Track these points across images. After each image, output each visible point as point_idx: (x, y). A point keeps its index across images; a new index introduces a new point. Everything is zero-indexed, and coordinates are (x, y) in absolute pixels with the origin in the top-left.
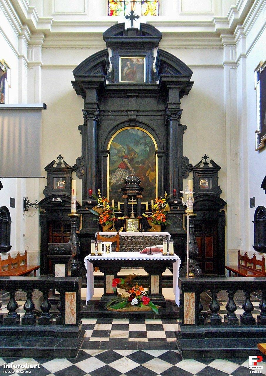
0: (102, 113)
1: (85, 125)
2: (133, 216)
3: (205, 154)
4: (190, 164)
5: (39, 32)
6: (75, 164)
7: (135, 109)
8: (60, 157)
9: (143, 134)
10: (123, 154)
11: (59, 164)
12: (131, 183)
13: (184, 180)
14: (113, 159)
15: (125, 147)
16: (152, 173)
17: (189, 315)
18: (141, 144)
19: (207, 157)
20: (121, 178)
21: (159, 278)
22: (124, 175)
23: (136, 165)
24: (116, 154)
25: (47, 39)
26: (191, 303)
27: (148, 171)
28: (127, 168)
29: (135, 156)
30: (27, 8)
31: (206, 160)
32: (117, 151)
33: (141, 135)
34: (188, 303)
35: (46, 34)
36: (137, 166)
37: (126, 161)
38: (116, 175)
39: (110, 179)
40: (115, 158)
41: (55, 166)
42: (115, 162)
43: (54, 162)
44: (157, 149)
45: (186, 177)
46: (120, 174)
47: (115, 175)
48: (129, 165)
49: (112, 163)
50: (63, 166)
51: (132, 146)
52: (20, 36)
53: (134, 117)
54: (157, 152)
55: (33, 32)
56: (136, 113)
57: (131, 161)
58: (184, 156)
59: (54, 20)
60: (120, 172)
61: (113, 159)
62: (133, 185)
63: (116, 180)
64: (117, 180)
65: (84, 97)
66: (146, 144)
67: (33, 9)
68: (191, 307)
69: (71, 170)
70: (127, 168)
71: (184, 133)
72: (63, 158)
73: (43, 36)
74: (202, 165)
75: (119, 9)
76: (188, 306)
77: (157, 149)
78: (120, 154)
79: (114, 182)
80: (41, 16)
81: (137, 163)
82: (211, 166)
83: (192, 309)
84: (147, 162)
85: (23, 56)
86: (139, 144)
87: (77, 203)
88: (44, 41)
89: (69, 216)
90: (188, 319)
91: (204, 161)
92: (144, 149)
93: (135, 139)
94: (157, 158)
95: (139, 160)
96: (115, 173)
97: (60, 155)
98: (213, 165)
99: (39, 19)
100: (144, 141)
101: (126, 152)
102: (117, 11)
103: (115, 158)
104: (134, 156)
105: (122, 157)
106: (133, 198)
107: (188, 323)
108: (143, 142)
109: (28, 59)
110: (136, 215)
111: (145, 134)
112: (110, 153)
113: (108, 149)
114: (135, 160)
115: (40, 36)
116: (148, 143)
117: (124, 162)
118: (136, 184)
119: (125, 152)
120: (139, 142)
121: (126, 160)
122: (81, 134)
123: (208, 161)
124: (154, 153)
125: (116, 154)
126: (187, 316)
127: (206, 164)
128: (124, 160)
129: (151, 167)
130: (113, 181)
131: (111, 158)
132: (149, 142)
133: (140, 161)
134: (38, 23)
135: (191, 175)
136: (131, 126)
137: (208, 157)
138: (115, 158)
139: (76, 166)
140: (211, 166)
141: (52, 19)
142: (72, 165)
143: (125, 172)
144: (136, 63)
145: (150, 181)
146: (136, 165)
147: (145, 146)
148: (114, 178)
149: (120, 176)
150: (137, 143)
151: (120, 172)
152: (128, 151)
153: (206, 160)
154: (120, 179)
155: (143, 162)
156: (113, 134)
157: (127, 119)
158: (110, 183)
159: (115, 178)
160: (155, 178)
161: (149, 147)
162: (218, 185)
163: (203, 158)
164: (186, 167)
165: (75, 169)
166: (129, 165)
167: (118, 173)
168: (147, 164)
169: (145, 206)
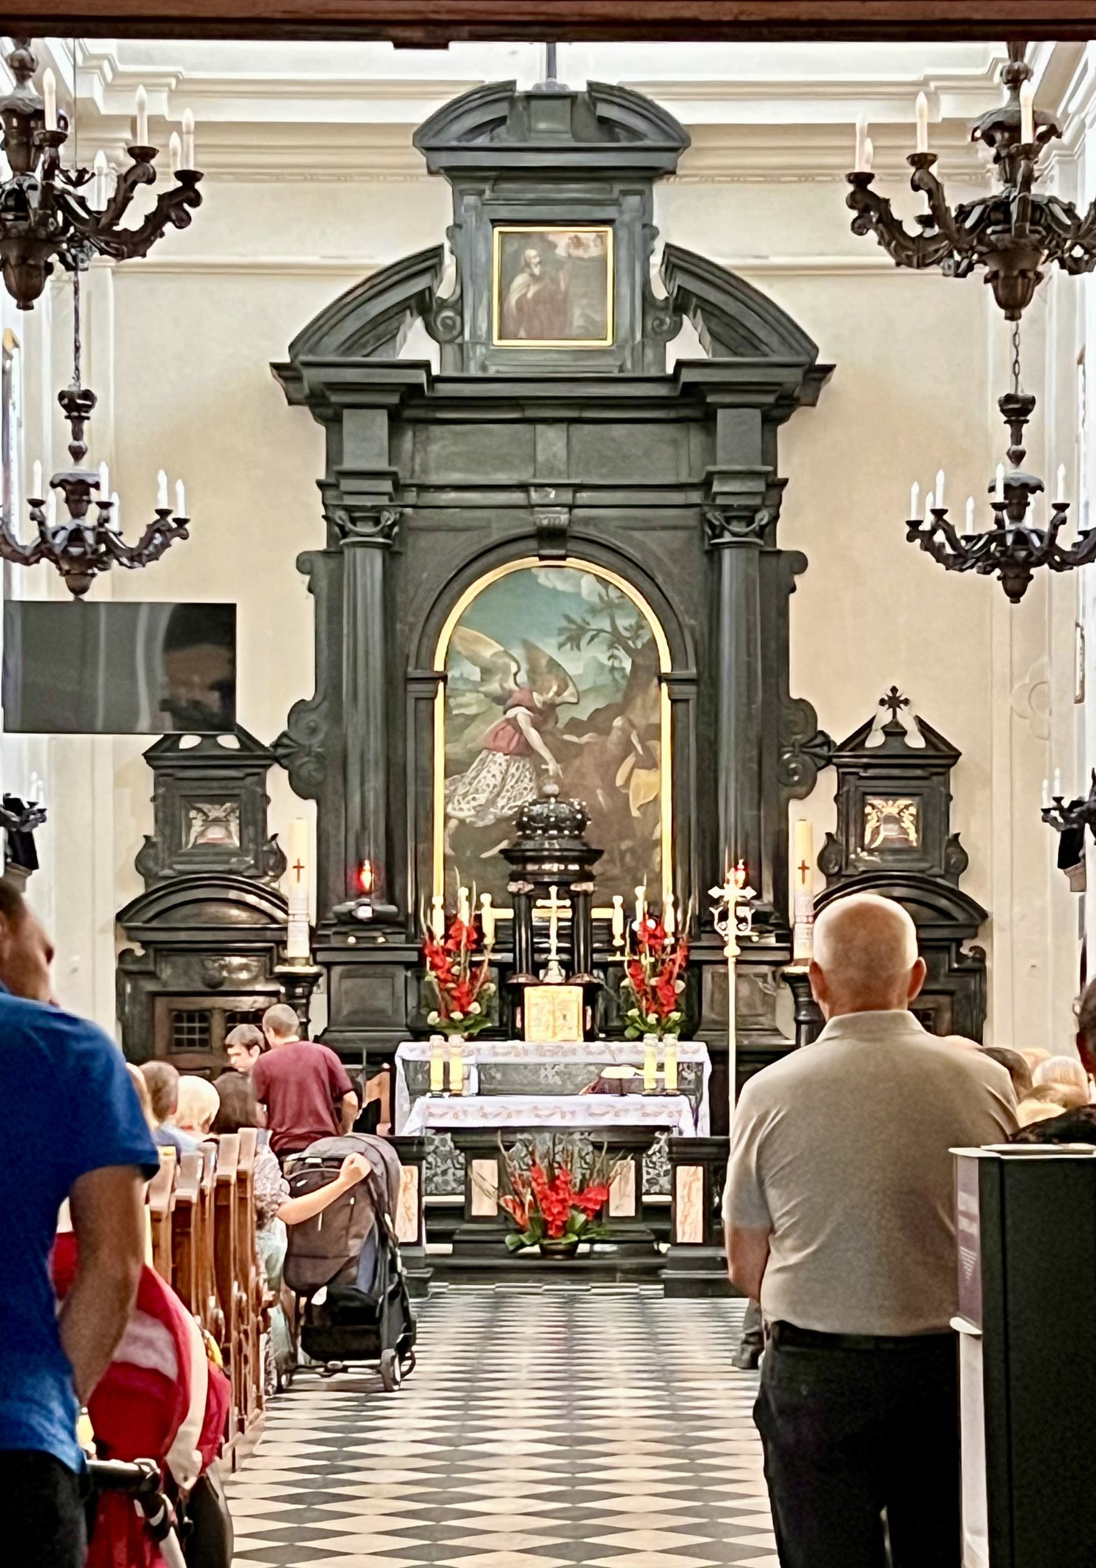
0: (411, 497)
4: (822, 733)
6: (284, 735)
9: (603, 592)
10: (506, 685)
12: (545, 830)
13: (795, 808)
14: (460, 706)
15: (518, 652)
16: (641, 775)
18: (592, 639)
19: (901, 702)
20: (498, 795)
22: (510, 782)
23: (567, 737)
24: (475, 687)
29: (566, 694)
32: (478, 669)
33: (596, 600)
39: (448, 799)
42: (471, 719)
44: (666, 667)
46: (494, 776)
47: (470, 784)
48: (534, 737)
49: (455, 727)
53: (563, 518)
57: (543, 716)
60: (495, 769)
61: (460, 706)
62: (552, 838)
63: (473, 804)
66: (616, 640)
70: (525, 750)
74: (876, 740)
77: (666, 667)
78: (494, 687)
79: (461, 815)
81: (575, 726)
82: (916, 741)
84: (618, 722)
91: (885, 716)
94: (666, 704)
95: (583, 714)
96: (471, 773)
100: (606, 625)
101: (522, 678)
103: (468, 705)
104: (558, 694)
105: (502, 700)
108: (603, 631)
111: (613, 594)
113: (439, 666)
114: (564, 715)
117: (513, 722)
120: (582, 630)
121: (521, 714)
124: (655, 681)
125: (475, 687)
127: (895, 731)
128: (511, 714)
130: (461, 809)
131: (452, 702)
133: (585, 718)
136: (542, 558)
137: (906, 702)
138: (470, 703)
139: (285, 741)
140: (916, 741)
143: (517, 769)
145: (635, 813)
146: (567, 737)
147: (611, 646)
148: (465, 795)
149: (495, 786)
150: (574, 637)
152: (532, 672)
154: (492, 802)
155: (598, 722)
158: (447, 818)
159: (470, 797)
160: (656, 800)
161: (629, 651)
163: (882, 702)
164: (803, 746)
166: (534, 737)
167: (484, 773)
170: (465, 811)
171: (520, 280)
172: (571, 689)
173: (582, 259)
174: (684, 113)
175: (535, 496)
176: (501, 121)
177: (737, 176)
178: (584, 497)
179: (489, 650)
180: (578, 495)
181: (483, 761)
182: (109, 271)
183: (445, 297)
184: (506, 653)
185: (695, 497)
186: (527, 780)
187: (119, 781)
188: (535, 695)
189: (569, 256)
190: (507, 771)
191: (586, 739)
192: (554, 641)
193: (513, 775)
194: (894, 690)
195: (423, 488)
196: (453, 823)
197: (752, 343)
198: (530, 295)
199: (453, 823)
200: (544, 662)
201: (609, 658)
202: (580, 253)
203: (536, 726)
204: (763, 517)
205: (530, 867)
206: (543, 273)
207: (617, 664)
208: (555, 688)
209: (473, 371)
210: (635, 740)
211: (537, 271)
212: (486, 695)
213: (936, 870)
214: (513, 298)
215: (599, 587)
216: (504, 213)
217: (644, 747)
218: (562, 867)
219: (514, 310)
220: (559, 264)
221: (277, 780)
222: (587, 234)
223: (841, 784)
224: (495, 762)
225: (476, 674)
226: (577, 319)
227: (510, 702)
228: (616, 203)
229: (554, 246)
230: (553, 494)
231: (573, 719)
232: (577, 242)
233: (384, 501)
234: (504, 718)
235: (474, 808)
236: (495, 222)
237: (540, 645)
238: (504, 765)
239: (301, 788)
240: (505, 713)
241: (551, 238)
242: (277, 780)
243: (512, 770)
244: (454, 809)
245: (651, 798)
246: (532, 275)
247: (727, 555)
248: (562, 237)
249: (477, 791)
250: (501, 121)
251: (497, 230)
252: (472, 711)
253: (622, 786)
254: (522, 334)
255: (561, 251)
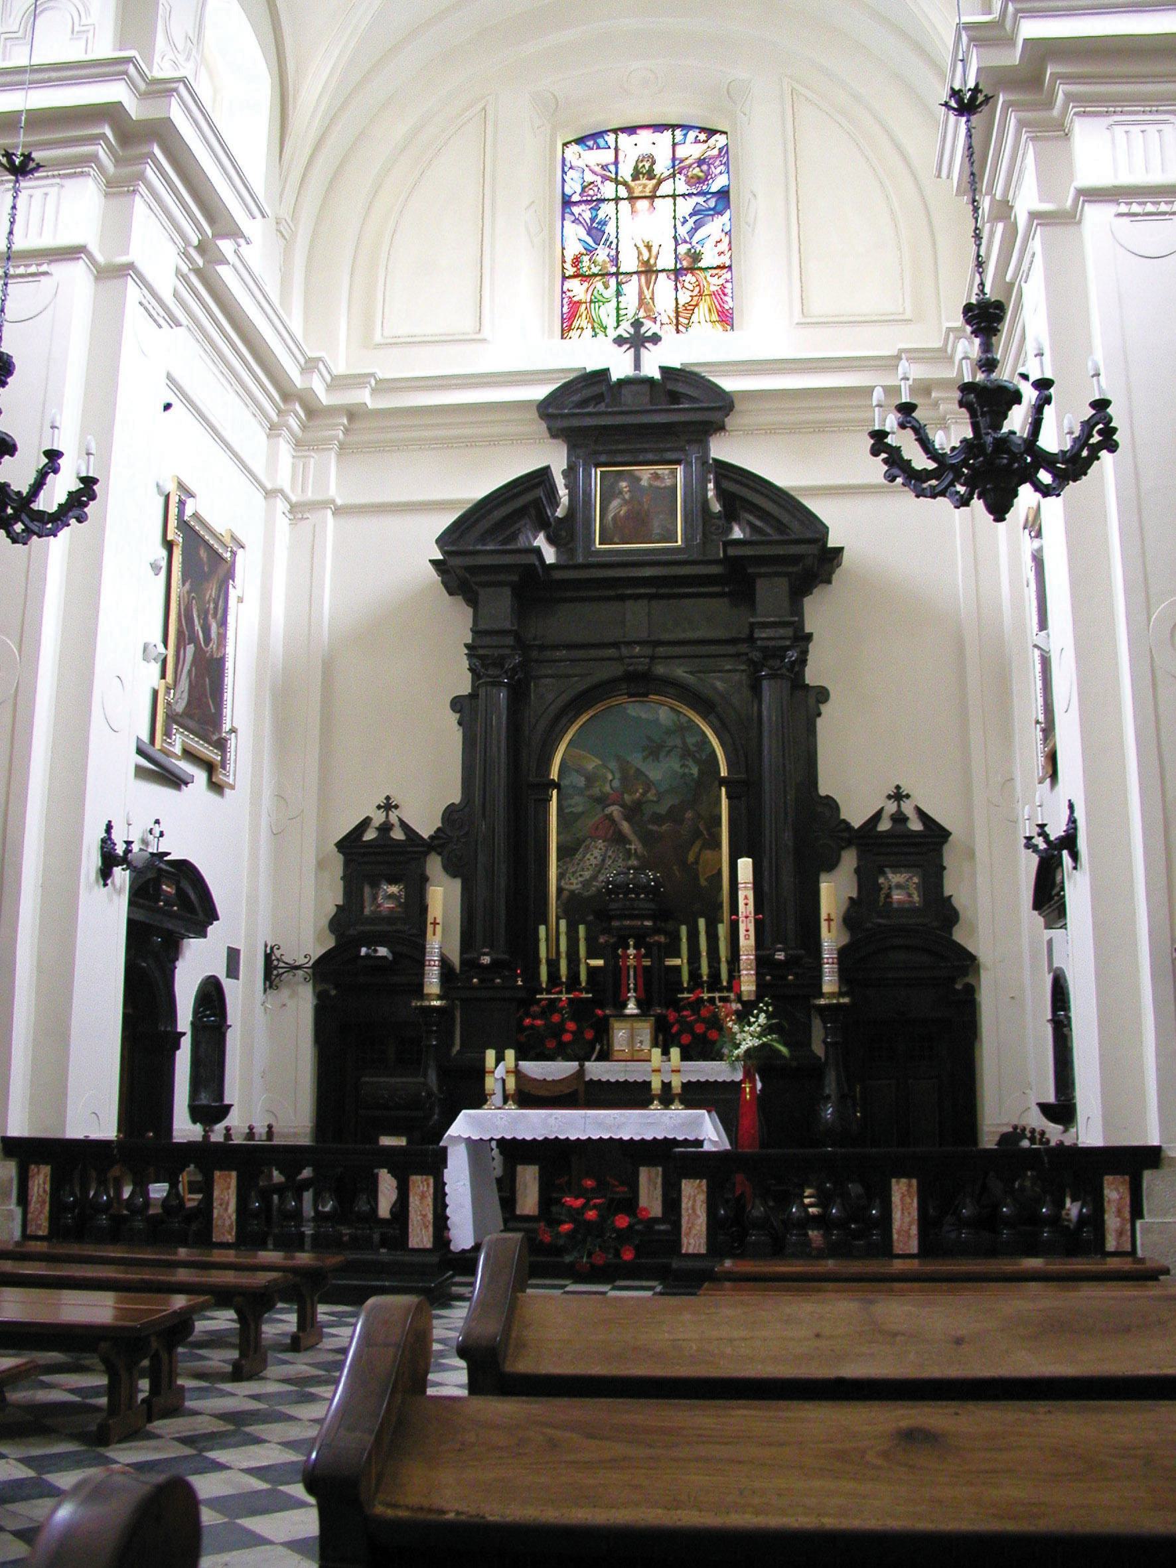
0: (534, 654)
1: (473, 696)
2: (632, 1008)
3: (895, 785)
4: (844, 821)
5: (332, 411)
6: (439, 829)
7: (644, 635)
8: (388, 806)
9: (675, 718)
11: (385, 828)
12: (626, 894)
14: (570, 806)
15: (613, 765)
16: (708, 854)
17: (694, 1232)
18: (669, 751)
19: (904, 796)
20: (599, 872)
21: (660, 1173)
23: (650, 827)
24: (581, 792)
25: (358, 425)
26: (699, 1203)
27: (696, 848)
28: (619, 839)
29: (649, 795)
30: (302, 361)
31: (899, 806)
32: (583, 779)
34: (690, 1204)
35: (353, 414)
36: (655, 828)
37: (615, 814)
38: (581, 864)
39: (560, 877)
40: (578, 804)
41: (370, 835)
42: (578, 816)
43: (365, 823)
44: (724, 772)
45: (831, 865)
46: (595, 858)
47: (578, 864)
48: (625, 827)
50: (398, 834)
51: (636, 760)
52: (273, 429)
54: (723, 782)
55: (313, 411)
56: (648, 651)
57: (633, 812)
58: (823, 791)
59: (380, 375)
60: (596, 852)
61: (570, 806)
62: (632, 899)
64: (586, 880)
65: (472, 600)
66: (686, 754)
67: (320, 359)
68: (699, 1212)
69: (425, 849)
70: (619, 839)
71: (819, 714)
72: (396, 807)
73: (345, 421)
74: (885, 826)
75: (600, 298)
76: (690, 1211)
77: (724, 772)
78: (596, 791)
79: (573, 887)
80: (340, 369)
81: (658, 819)
82: (916, 825)
83: (699, 1217)
84: (689, 815)
85: (281, 491)
86: (662, 754)
87: (445, 963)
88: (347, 431)
89: (416, 1008)
90: (692, 1241)
91: (891, 807)
92: (681, 771)
93: (649, 738)
94: (724, 802)
95: (662, 809)
96: (578, 856)
97: (388, 798)
98: (924, 824)
99: (334, 378)
100: (678, 742)
101: (616, 783)
102: (593, 305)
103: (576, 805)
104: (644, 794)
105: (602, 801)
106: (631, 943)
107: (690, 1251)
108: (676, 747)
109: (293, 492)
110: (639, 1004)
111: (683, 720)
112: (557, 786)
113: (554, 775)
115: (335, 421)
116: (693, 748)
117: (609, 817)
118: (642, 896)
119: (610, 782)
120: (660, 747)
121: (615, 810)
122: (460, 723)
123: (908, 808)
124: (717, 783)
125: (581, 792)
126: (688, 1234)
127: (899, 819)
129: (705, 832)
130: (572, 884)
131: (565, 803)
132: (695, 745)
134: (330, 388)
135: (849, 860)
136: (631, 696)
137: (908, 796)
138: (578, 804)
139: (441, 835)
140: (916, 825)
141: (373, 375)
142: (426, 832)
144: (651, 486)
145: (703, 883)
146: (650, 827)
147: (683, 757)
148: (574, 873)
149: (596, 865)
150: (654, 751)
151: (595, 854)
152: (624, 779)
153: (899, 806)
154: (594, 877)
155: (674, 815)
156: (572, 722)
157: (617, 670)
158: (560, 890)
159: (578, 874)
161: (697, 762)
162: (947, 893)
163: (889, 797)
165: (437, 843)
166: (625, 827)
167: (588, 856)
168: (690, 823)
169: (678, 969)
170: (575, 885)
171: (615, 503)
172: (653, 791)
173: (658, 488)
174: (728, 384)
175: (625, 651)
176: (599, 398)
177: (771, 431)
178: (661, 650)
179: (592, 764)
180: (657, 649)
181: (588, 848)
182: (329, 512)
183: (560, 516)
184: (605, 766)
185: (743, 648)
186: (620, 860)
187: (321, 865)
188: (626, 796)
189: (651, 486)
190: (605, 854)
191: (664, 827)
192: (640, 756)
193: (610, 857)
194: (898, 787)
195: (542, 648)
196: (566, 894)
197: (781, 527)
198: (622, 512)
199: (566, 894)
200: (632, 772)
201: (681, 766)
202: (657, 483)
203: (627, 818)
204: (793, 655)
205: (615, 924)
206: (632, 498)
207: (687, 771)
208: (641, 791)
209: (581, 560)
210: (702, 828)
211: (627, 496)
212: (590, 797)
213: (935, 924)
214: (610, 516)
215: (673, 715)
216: (603, 458)
217: (710, 834)
218: (639, 923)
219: (611, 526)
220: (641, 489)
221: (434, 865)
222: (662, 470)
223: (859, 858)
224: (596, 848)
225: (581, 782)
226: (656, 527)
227: (608, 802)
228: (682, 450)
229: (639, 479)
230: (638, 649)
231: (655, 813)
232: (656, 476)
233: (508, 651)
234: (601, 815)
235: (581, 882)
236: (597, 465)
237: (629, 759)
238: (604, 849)
239: (452, 869)
240: (603, 810)
241: (637, 473)
242: (434, 865)
243: (610, 853)
244: (566, 884)
245: (715, 872)
246: (624, 499)
247: (765, 683)
248: (645, 473)
249: (583, 870)
250: (599, 398)
251: (598, 470)
252: (580, 809)
253: (692, 863)
254: (616, 540)
255: (644, 483)
